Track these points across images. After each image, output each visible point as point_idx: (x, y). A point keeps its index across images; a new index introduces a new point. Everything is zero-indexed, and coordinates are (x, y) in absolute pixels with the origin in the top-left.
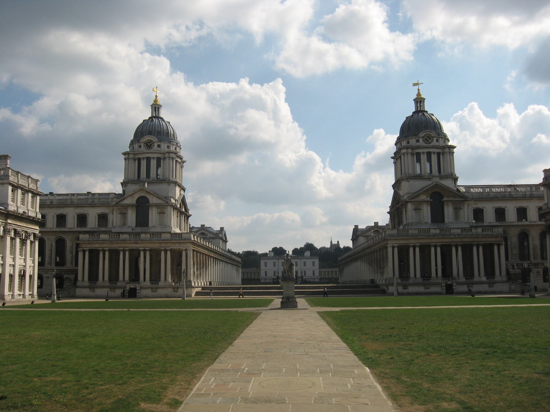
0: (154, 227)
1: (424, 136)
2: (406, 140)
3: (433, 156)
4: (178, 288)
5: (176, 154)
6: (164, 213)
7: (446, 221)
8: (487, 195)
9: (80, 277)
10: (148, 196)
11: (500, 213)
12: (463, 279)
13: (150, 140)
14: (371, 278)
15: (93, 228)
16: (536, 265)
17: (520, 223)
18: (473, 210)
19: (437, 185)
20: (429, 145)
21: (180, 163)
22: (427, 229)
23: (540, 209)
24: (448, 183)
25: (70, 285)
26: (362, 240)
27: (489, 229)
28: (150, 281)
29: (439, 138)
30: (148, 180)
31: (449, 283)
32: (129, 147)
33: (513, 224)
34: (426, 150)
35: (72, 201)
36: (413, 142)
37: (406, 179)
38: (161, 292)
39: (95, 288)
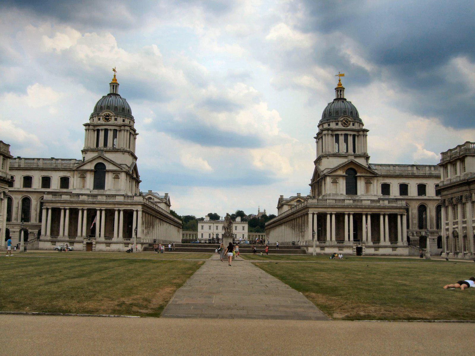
0: (109, 190)
1: (342, 120)
2: (327, 123)
3: (349, 137)
4: (128, 244)
5: (130, 127)
7: (359, 193)
8: (394, 173)
9: (43, 232)
10: (106, 164)
11: (404, 189)
12: (371, 243)
13: (108, 114)
14: (293, 241)
15: (56, 190)
16: (432, 233)
17: (421, 197)
18: (382, 185)
19: (352, 162)
20: (347, 128)
21: (133, 135)
22: (343, 199)
23: (437, 186)
24: (361, 161)
25: (34, 239)
26: (286, 208)
27: (394, 201)
28: (105, 237)
29: (355, 122)
30: (105, 149)
31: (359, 246)
32: (90, 120)
33: (414, 198)
34: (344, 133)
35: (38, 164)
36: (333, 125)
37: (324, 157)
38: (114, 247)
39: (55, 242)
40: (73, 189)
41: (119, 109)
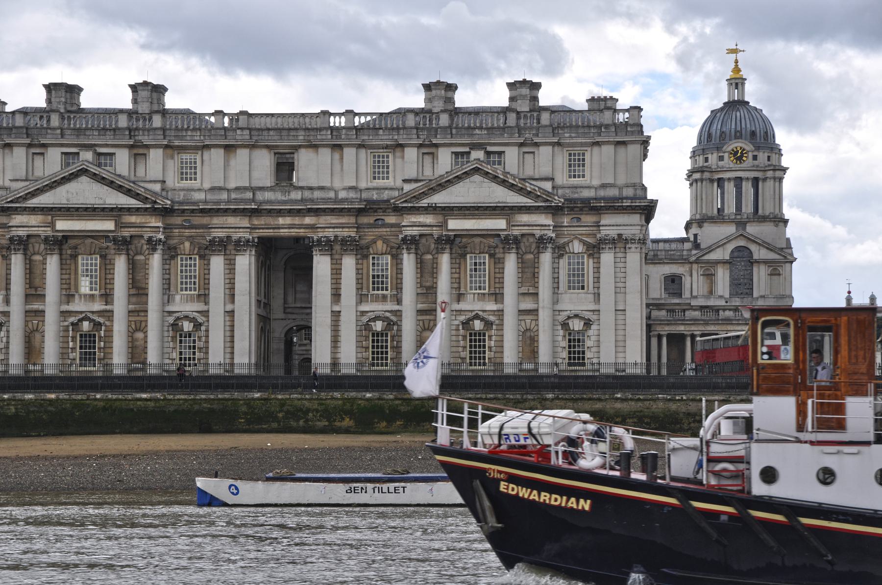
0: (763, 297)
6: (779, 275)
10: (753, 248)
40: (689, 296)
41: (758, 135)
